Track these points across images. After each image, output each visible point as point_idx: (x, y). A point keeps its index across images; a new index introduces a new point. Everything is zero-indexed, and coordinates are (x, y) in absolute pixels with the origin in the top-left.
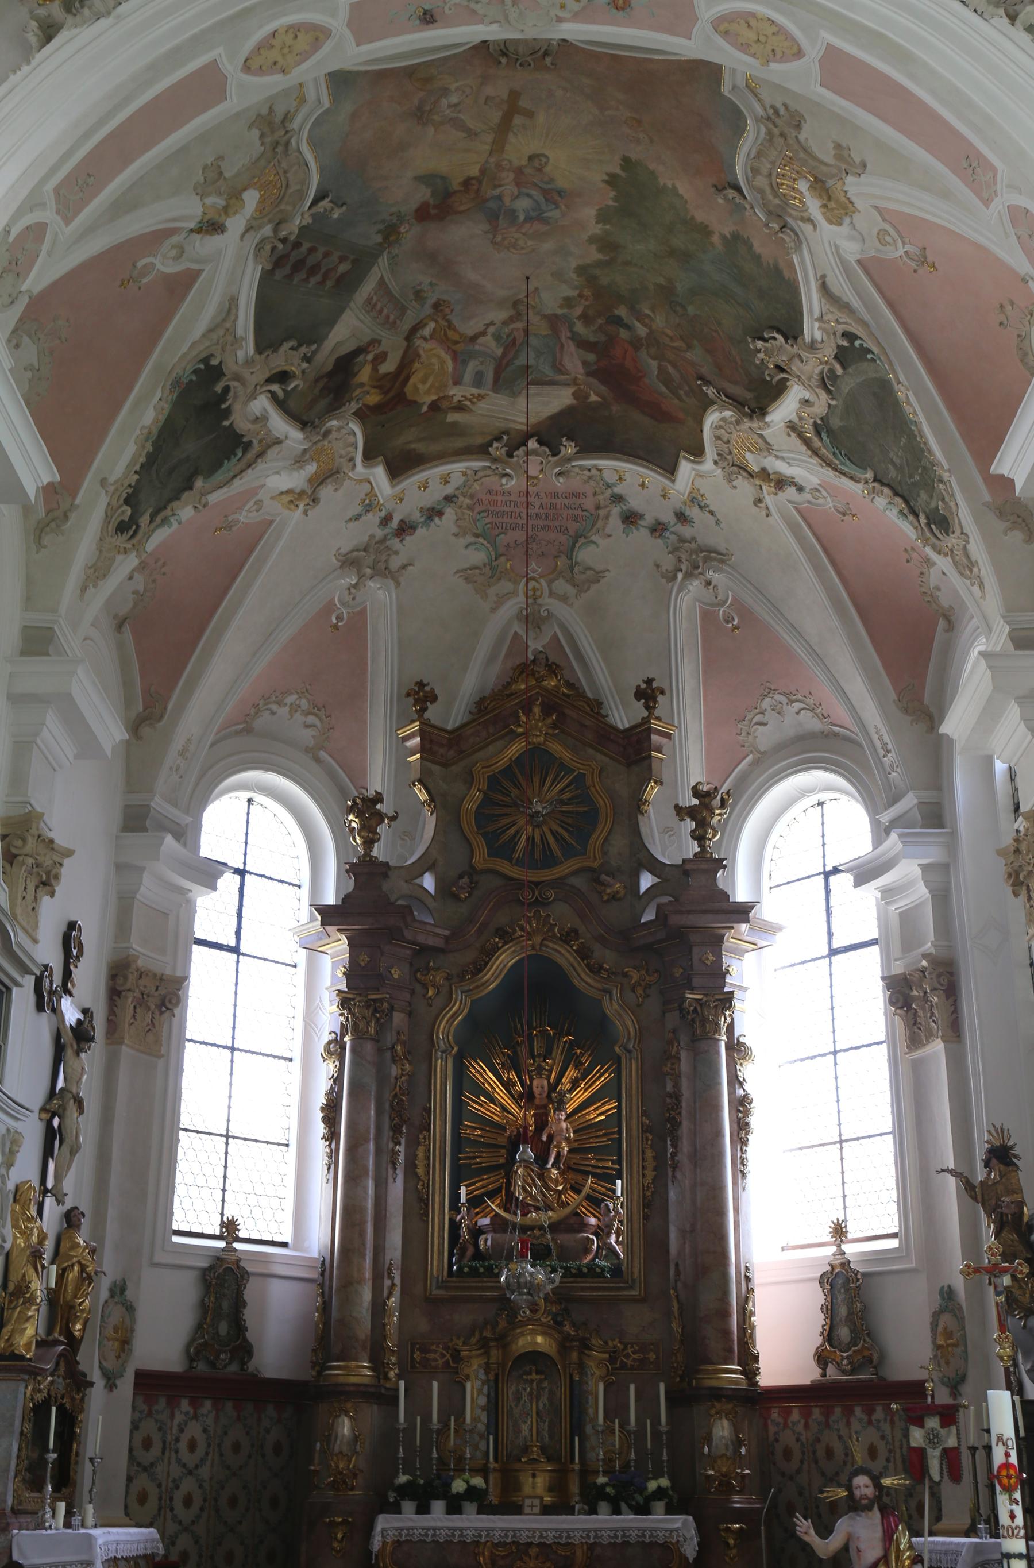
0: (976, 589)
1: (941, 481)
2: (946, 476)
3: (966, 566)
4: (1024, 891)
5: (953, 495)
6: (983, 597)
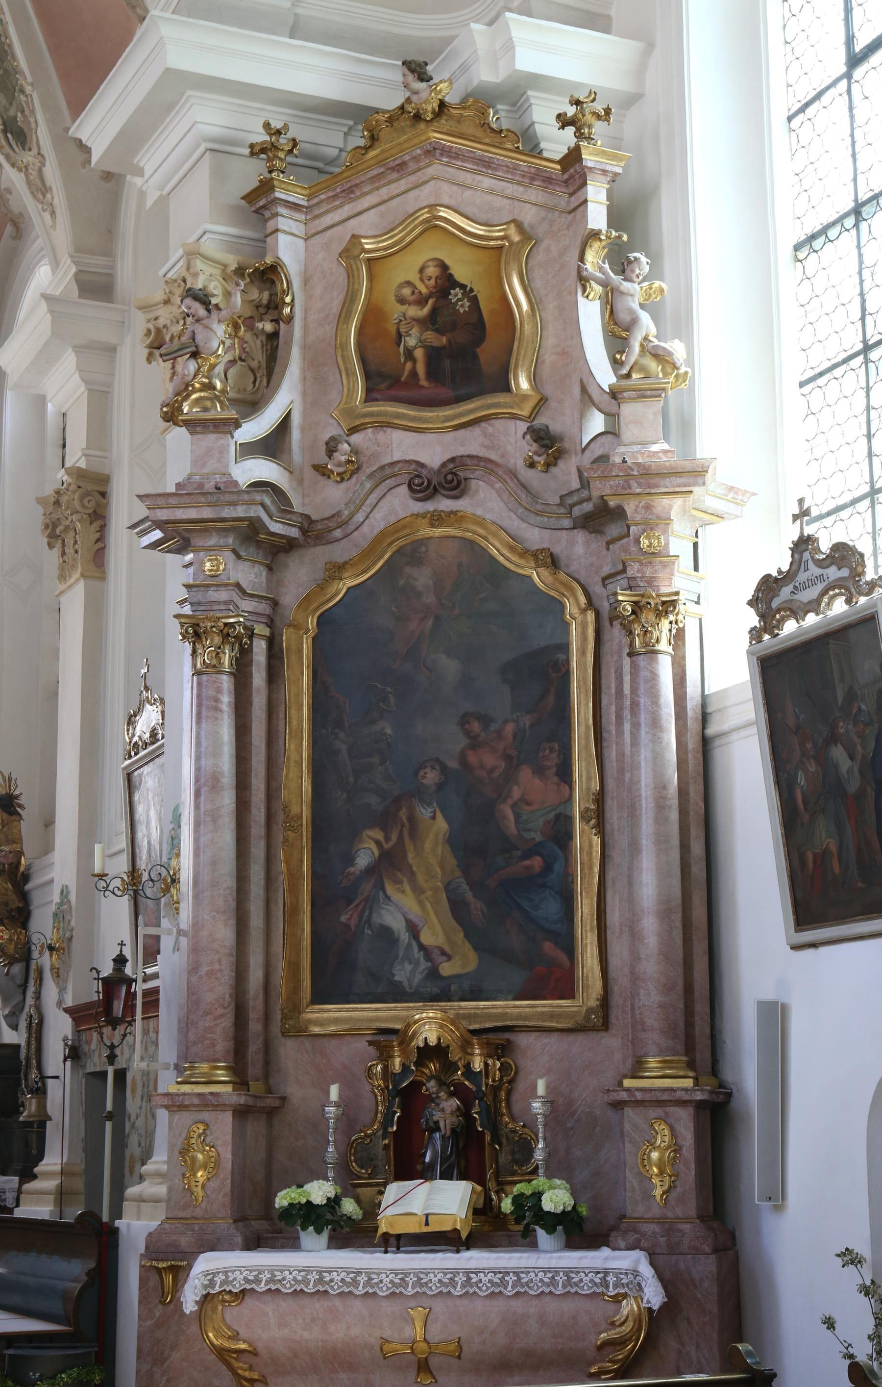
0: (47, 216)
1: (22, 91)
2: (28, 89)
3: (40, 190)
4: (59, 544)
5: (33, 112)
6: (54, 226)
